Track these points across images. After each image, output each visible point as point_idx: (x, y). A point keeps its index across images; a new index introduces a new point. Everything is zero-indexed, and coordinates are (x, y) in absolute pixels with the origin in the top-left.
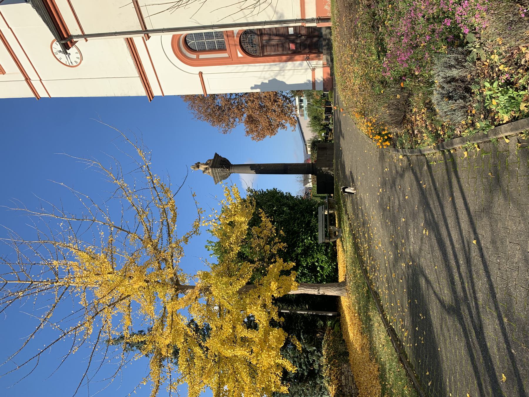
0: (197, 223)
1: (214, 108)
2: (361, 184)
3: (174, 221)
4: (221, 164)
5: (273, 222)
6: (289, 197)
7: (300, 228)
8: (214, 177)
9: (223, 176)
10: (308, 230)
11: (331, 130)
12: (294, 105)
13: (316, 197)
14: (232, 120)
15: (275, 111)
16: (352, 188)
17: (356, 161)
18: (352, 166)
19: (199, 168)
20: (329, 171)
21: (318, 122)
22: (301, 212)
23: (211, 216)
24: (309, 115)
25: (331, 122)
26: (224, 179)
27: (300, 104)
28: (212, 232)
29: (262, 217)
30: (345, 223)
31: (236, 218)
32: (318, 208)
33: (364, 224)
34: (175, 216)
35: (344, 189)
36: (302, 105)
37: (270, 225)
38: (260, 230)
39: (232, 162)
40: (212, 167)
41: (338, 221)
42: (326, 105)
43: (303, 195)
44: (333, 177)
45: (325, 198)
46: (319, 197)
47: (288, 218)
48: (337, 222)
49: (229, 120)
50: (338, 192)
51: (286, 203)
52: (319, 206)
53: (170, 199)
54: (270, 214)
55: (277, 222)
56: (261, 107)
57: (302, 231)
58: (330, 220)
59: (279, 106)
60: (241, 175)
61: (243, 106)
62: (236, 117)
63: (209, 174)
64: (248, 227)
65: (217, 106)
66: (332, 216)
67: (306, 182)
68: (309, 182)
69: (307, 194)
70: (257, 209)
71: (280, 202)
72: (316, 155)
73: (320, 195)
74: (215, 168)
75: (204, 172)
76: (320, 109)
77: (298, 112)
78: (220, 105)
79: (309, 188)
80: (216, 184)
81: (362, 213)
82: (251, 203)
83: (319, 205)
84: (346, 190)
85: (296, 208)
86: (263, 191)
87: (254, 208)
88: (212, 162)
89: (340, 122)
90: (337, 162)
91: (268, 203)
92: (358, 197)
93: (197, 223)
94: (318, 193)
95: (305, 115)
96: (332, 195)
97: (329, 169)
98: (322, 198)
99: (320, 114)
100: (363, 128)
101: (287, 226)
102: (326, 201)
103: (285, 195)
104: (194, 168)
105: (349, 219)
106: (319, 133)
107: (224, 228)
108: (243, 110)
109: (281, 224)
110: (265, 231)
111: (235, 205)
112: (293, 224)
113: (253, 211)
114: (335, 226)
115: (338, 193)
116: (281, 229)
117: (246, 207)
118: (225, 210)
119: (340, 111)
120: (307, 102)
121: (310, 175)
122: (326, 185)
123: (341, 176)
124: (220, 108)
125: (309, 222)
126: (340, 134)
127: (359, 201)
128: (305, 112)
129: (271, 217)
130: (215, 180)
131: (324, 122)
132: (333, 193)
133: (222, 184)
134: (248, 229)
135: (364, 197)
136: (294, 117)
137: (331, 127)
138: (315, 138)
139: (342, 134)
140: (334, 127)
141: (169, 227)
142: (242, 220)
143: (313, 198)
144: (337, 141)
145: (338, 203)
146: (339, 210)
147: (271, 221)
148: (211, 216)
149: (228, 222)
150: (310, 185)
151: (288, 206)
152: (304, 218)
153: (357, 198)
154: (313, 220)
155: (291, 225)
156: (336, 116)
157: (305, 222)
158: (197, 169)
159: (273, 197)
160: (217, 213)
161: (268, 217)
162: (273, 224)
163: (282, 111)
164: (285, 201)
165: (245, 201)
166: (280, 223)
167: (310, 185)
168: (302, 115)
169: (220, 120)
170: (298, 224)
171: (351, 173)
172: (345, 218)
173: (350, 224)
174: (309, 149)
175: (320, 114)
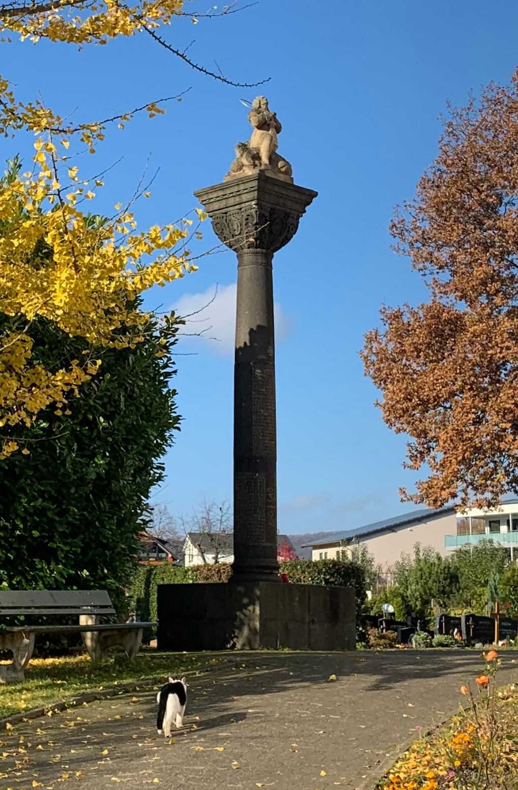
0: (44, 122)
1: (492, 187)
2: (197, 755)
3: (53, 32)
4: (274, 213)
5: (47, 414)
6: (145, 477)
7: (24, 521)
8: (222, 187)
9: (229, 223)
10: (18, 551)
11: (405, 638)
12: (501, 497)
13: (148, 583)
14: (444, 255)
15: (477, 422)
16: (179, 719)
17: (285, 737)
18: (266, 718)
19: (260, 127)
20: (246, 631)
21: (435, 588)
22: (89, 524)
23: (72, 174)
24: (462, 554)
25: (438, 638)
26: (215, 225)
27: (505, 519)
28: (11, 178)
29: (69, 371)
30: (44, 693)
31: (64, 274)
32: (102, 587)
33: (43, 767)
34: (75, 36)
35: (177, 689)
36: (503, 528)
37: (39, 402)
38: (20, 366)
39: (279, 257)
40: (262, 178)
41: (54, 666)
42: (503, 619)
43: (154, 530)
44: (223, 648)
45: (144, 614)
46: (147, 594)
47: (66, 475)
48: (49, 661)
49: (446, 244)
50: (168, 668)
51: (121, 465)
52: (110, 591)
53: (140, 18)
54: (78, 404)
55: (49, 432)
56: (494, 368)
57: (15, 527)
58: (58, 637)
59: (499, 437)
60: (233, 290)
61: (497, 300)
62: (454, 273)
63: (233, 166)
64: (30, 316)
65: (500, 198)
66: (72, 641)
67: (207, 541)
68: (202, 553)
69: (158, 546)
70: (98, 352)
71: (126, 441)
72: (309, 581)
73: (154, 597)
74: (260, 189)
75: (244, 147)
76: (487, 597)
77: (476, 512)
78: (501, 210)
79: (179, 556)
80: (198, 195)
81: (85, 760)
82: (123, 330)
83: (117, 594)
84: (173, 700)
85: (104, 504)
86: (168, 375)
87: (104, 341)
88: (282, 177)
89: (435, 674)
90: (282, 662)
91: (126, 397)
92: (148, 743)
93: (44, 122)
94: (161, 588)
95: (463, 539)
96: (154, 643)
97: (253, 631)
98: (143, 606)
99: (467, 595)
100: (412, 763)
101: (36, 469)
102: (132, 620)
103: (156, 461)
104: (258, 111)
105: (63, 708)
106: (395, 594)
107: (27, 224)
108: (483, 299)
109: (41, 445)
110: (15, 384)
111: (116, 269)
112: (41, 494)
113: (91, 336)
114: (34, 656)
115: (160, 666)
116: (22, 446)
117: (107, 312)
118: (94, 230)
119: (480, 673)
120: (512, 545)
121: (231, 559)
122: (194, 620)
123: (226, 679)
124: (490, 209)
125: (50, 555)
126: (389, 673)
127: (128, 747)
128: (474, 540)
129: (71, 406)
130: (214, 189)
131: (436, 611)
132: (160, 648)
133: (198, 217)
134: (22, 320)
135: (146, 766)
136: (454, 496)
137: (418, 639)
138: (376, 578)
139: (388, 681)
140: (417, 652)
141: (31, 12)
142: (57, 296)
143: (142, 571)
144: (363, 662)
145: (124, 666)
146: (97, 672)
147: (53, 406)
148: (72, 174)
149: (48, 240)
150: (193, 558)
151: (112, 474)
152: (63, 535)
153: (141, 738)
154: (56, 571)
155: (37, 486)
156: (458, 659)
157: (51, 539)
158: (254, 123)
159: (147, 416)
160: (84, 197)
161: (69, 394)
162: (42, 415)
163: (477, 450)
164: (131, 463)
165: (131, 305)
166: (43, 444)
167: (193, 558)
168: (463, 528)
169: (443, 209)
170: (41, 512)
171: (240, 717)
172: (66, 694)
173: (42, 713)
174: (331, 554)
175: (467, 595)
